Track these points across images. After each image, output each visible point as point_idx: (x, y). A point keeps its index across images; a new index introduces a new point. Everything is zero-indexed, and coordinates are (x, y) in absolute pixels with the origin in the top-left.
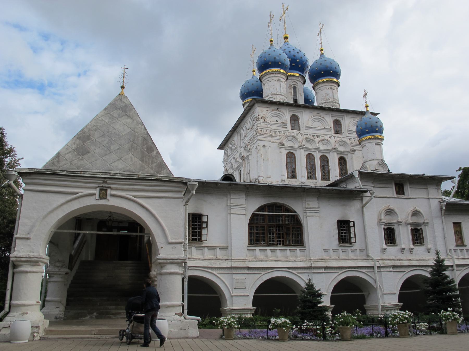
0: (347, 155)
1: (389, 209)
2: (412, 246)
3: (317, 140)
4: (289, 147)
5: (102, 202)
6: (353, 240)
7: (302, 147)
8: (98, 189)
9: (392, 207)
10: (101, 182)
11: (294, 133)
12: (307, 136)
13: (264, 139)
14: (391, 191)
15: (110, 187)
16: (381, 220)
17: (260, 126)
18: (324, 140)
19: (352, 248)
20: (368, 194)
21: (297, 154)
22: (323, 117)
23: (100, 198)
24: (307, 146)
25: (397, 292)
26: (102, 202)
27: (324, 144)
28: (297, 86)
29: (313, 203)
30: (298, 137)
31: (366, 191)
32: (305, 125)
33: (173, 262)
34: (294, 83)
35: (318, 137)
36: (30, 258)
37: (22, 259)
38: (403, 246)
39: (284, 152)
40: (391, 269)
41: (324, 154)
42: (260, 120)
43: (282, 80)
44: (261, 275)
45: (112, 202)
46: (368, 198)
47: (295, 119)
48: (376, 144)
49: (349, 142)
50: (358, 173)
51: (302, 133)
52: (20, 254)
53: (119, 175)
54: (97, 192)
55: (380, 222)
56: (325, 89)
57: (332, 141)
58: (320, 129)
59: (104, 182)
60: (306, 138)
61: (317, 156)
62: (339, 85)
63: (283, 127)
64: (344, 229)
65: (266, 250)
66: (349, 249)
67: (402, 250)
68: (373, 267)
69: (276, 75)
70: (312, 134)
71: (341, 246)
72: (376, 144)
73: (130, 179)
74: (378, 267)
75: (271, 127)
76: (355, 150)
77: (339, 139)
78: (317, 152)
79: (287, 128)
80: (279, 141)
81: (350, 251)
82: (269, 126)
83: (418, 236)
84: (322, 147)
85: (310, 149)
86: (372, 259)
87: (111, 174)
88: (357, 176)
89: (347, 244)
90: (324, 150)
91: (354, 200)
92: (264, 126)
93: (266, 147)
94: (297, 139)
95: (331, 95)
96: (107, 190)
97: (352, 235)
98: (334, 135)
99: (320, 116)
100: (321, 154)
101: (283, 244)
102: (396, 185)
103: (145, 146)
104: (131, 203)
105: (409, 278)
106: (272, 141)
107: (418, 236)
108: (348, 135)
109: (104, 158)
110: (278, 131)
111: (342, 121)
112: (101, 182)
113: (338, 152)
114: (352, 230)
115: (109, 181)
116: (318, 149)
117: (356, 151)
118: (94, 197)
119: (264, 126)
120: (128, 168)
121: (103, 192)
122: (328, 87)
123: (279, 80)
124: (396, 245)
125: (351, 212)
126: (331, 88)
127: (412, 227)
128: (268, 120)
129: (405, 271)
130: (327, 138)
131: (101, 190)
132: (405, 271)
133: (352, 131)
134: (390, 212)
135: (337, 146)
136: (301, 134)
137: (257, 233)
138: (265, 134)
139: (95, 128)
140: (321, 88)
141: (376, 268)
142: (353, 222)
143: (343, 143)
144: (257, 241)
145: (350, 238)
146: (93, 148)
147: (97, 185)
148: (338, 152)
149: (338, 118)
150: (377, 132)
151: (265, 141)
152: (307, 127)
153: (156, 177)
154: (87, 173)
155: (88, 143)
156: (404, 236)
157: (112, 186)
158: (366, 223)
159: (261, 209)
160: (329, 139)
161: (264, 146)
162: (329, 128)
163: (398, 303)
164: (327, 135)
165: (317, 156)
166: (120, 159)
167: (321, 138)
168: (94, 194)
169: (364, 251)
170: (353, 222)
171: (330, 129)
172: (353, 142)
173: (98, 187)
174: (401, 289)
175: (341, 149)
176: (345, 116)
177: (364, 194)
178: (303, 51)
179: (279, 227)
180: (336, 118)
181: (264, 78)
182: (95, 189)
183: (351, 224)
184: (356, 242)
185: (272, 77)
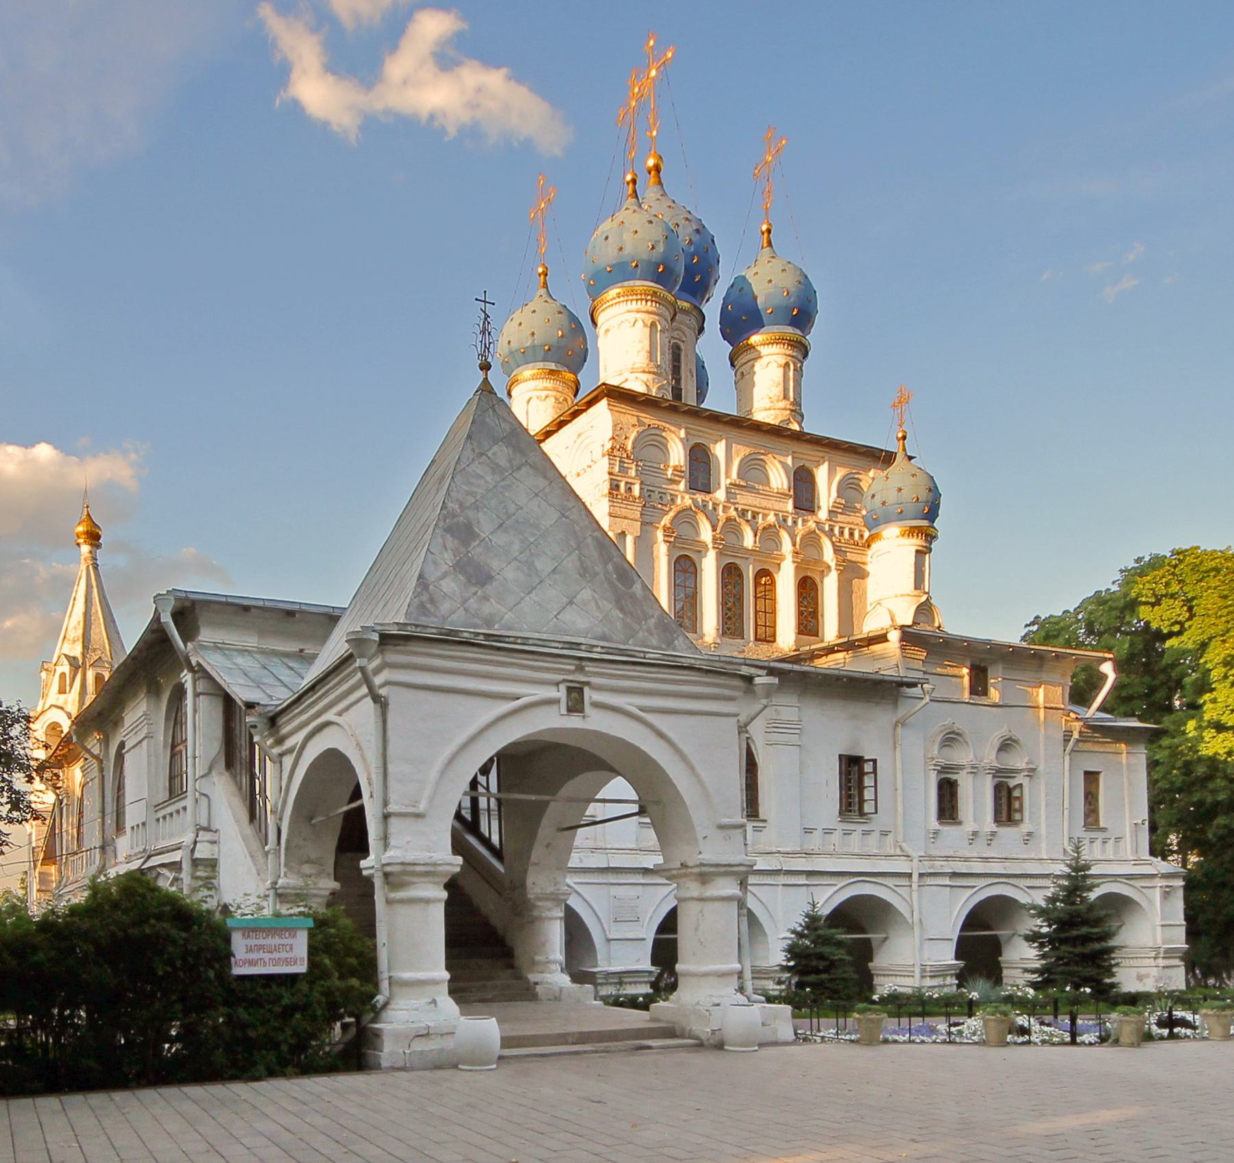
2: (993, 827)
5: (574, 722)
8: (563, 687)
10: (573, 668)
15: (588, 683)
20: (916, 691)
23: (570, 710)
26: (574, 722)
33: (726, 870)
36: (435, 864)
37: (418, 869)
45: (595, 721)
52: (410, 857)
53: (599, 650)
54: (562, 693)
59: (580, 669)
73: (634, 663)
83: (1007, 805)
87: (583, 647)
96: (582, 690)
97: (868, 794)
103: (610, 567)
104: (634, 725)
107: (1007, 805)
109: (533, 595)
112: (573, 668)
114: (868, 781)
115: (590, 667)
118: (555, 707)
120: (600, 630)
121: (574, 695)
124: (960, 823)
125: (867, 732)
131: (569, 690)
139: (471, 500)
142: (875, 761)
146: (495, 564)
147: (561, 677)
153: (683, 660)
154: (531, 642)
155: (476, 550)
156: (976, 798)
157: (595, 680)
166: (571, 603)
168: (556, 701)
170: (875, 761)
173: (564, 681)
182: (555, 688)
183: (868, 768)
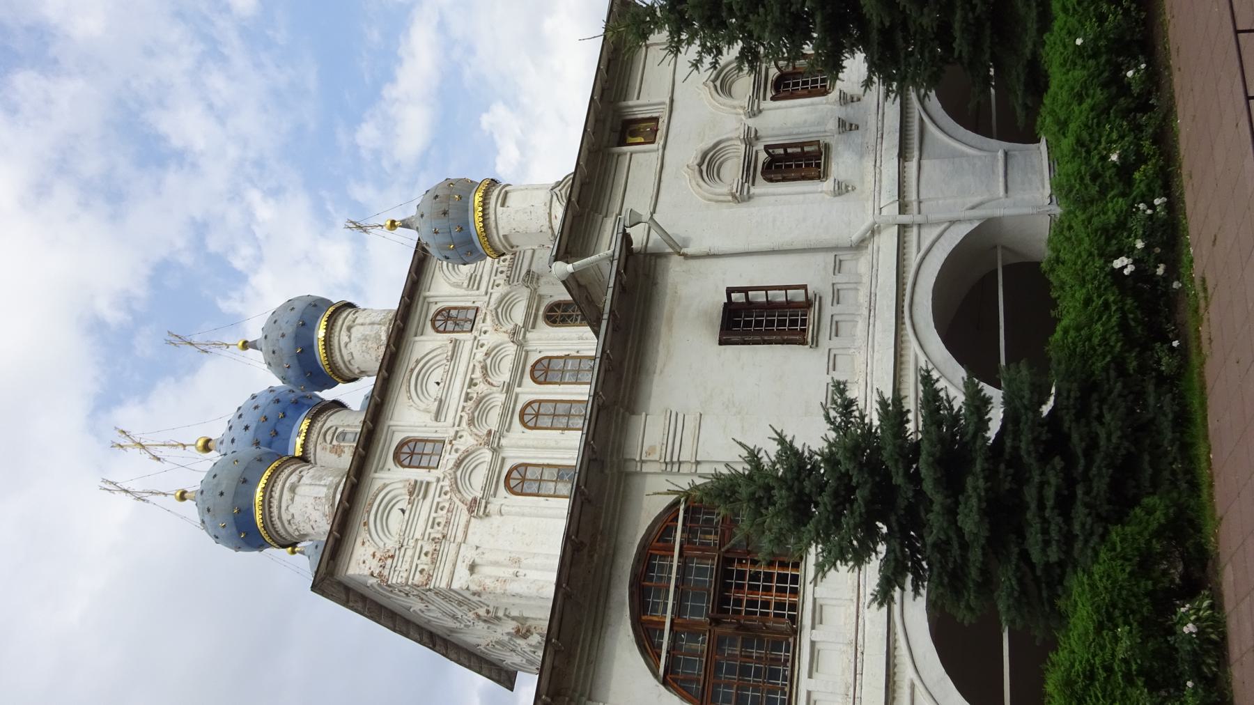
0: (540, 297)
1: (700, 165)
3: (482, 388)
4: (489, 480)
6: (799, 296)
7: (493, 442)
9: (693, 157)
11: (449, 459)
12: (466, 418)
13: (449, 566)
14: (639, 163)
16: (734, 196)
17: (405, 575)
18: (484, 368)
19: (827, 300)
21: (514, 456)
22: (418, 362)
24: (493, 421)
25: (999, 147)
27: (496, 366)
28: (340, 430)
29: (649, 434)
30: (463, 448)
31: (627, 239)
32: (428, 419)
34: (328, 438)
35: (472, 383)
38: (832, 125)
39: (502, 498)
40: (912, 166)
41: (528, 369)
42: (386, 573)
43: (294, 478)
44: (919, 688)
46: (654, 235)
47: (409, 453)
48: (503, 205)
49: (503, 289)
50: (559, 263)
51: (452, 434)
55: (740, 197)
56: (351, 346)
57: (490, 339)
58: (451, 374)
60: (471, 422)
61: (530, 391)
62: (350, 305)
63: (424, 497)
64: (755, 320)
65: (813, 643)
66: (828, 310)
67: (845, 126)
68: (903, 228)
69: (276, 495)
70: (462, 403)
71: (815, 343)
72: (503, 205)
74: (903, 208)
75: (418, 535)
76: (528, 272)
77: (489, 318)
78: (517, 390)
79: (428, 483)
80: (465, 515)
81: (837, 309)
82: (412, 543)
84: (505, 376)
85: (506, 413)
86: (874, 231)
88: (570, 268)
89: (812, 316)
90: (514, 370)
91: (655, 284)
92: (408, 558)
93: (478, 561)
94: (468, 453)
95: (367, 330)
98: (475, 333)
99: (412, 370)
100: (527, 379)
101: (796, 566)
102: (623, 142)
105: (944, 107)
106: (460, 538)
108: (483, 288)
110: (433, 515)
111: (441, 305)
113: (530, 323)
116: (508, 388)
117: (533, 268)
119: (408, 558)
122: (344, 339)
123: (293, 489)
126: (349, 329)
127: (769, 95)
128: (391, 544)
129: (921, 120)
130: (480, 355)
132: (921, 120)
133: (471, 278)
134: (709, 164)
135: (510, 327)
136: (457, 436)
137: (745, 671)
138: (434, 562)
140: (346, 358)
141: (905, 219)
142: (730, 291)
143: (504, 305)
144: (774, 674)
145: (789, 304)
148: (530, 323)
149: (430, 316)
150: (464, 199)
151: (454, 565)
152: (437, 418)
158: (740, 246)
159: (647, 641)
160: (485, 349)
161: (472, 568)
162: (450, 347)
163: (1043, 145)
164: (472, 355)
165: (530, 391)
167: (478, 374)
169: (841, 253)
170: (730, 291)
171: (455, 343)
172: (504, 276)
174: (988, 134)
175: (519, 314)
176: (427, 294)
177: (637, 244)
178: (243, 399)
179: (729, 574)
180: (429, 324)
181: (282, 532)
184: (804, 287)
185: (280, 507)
